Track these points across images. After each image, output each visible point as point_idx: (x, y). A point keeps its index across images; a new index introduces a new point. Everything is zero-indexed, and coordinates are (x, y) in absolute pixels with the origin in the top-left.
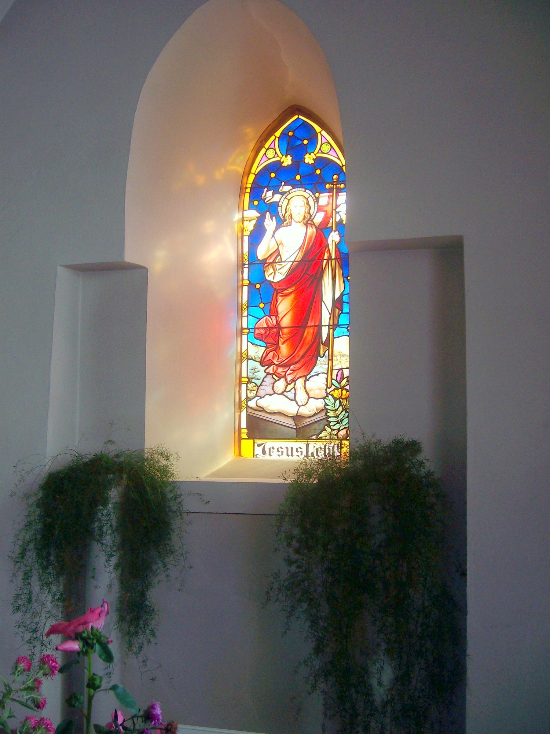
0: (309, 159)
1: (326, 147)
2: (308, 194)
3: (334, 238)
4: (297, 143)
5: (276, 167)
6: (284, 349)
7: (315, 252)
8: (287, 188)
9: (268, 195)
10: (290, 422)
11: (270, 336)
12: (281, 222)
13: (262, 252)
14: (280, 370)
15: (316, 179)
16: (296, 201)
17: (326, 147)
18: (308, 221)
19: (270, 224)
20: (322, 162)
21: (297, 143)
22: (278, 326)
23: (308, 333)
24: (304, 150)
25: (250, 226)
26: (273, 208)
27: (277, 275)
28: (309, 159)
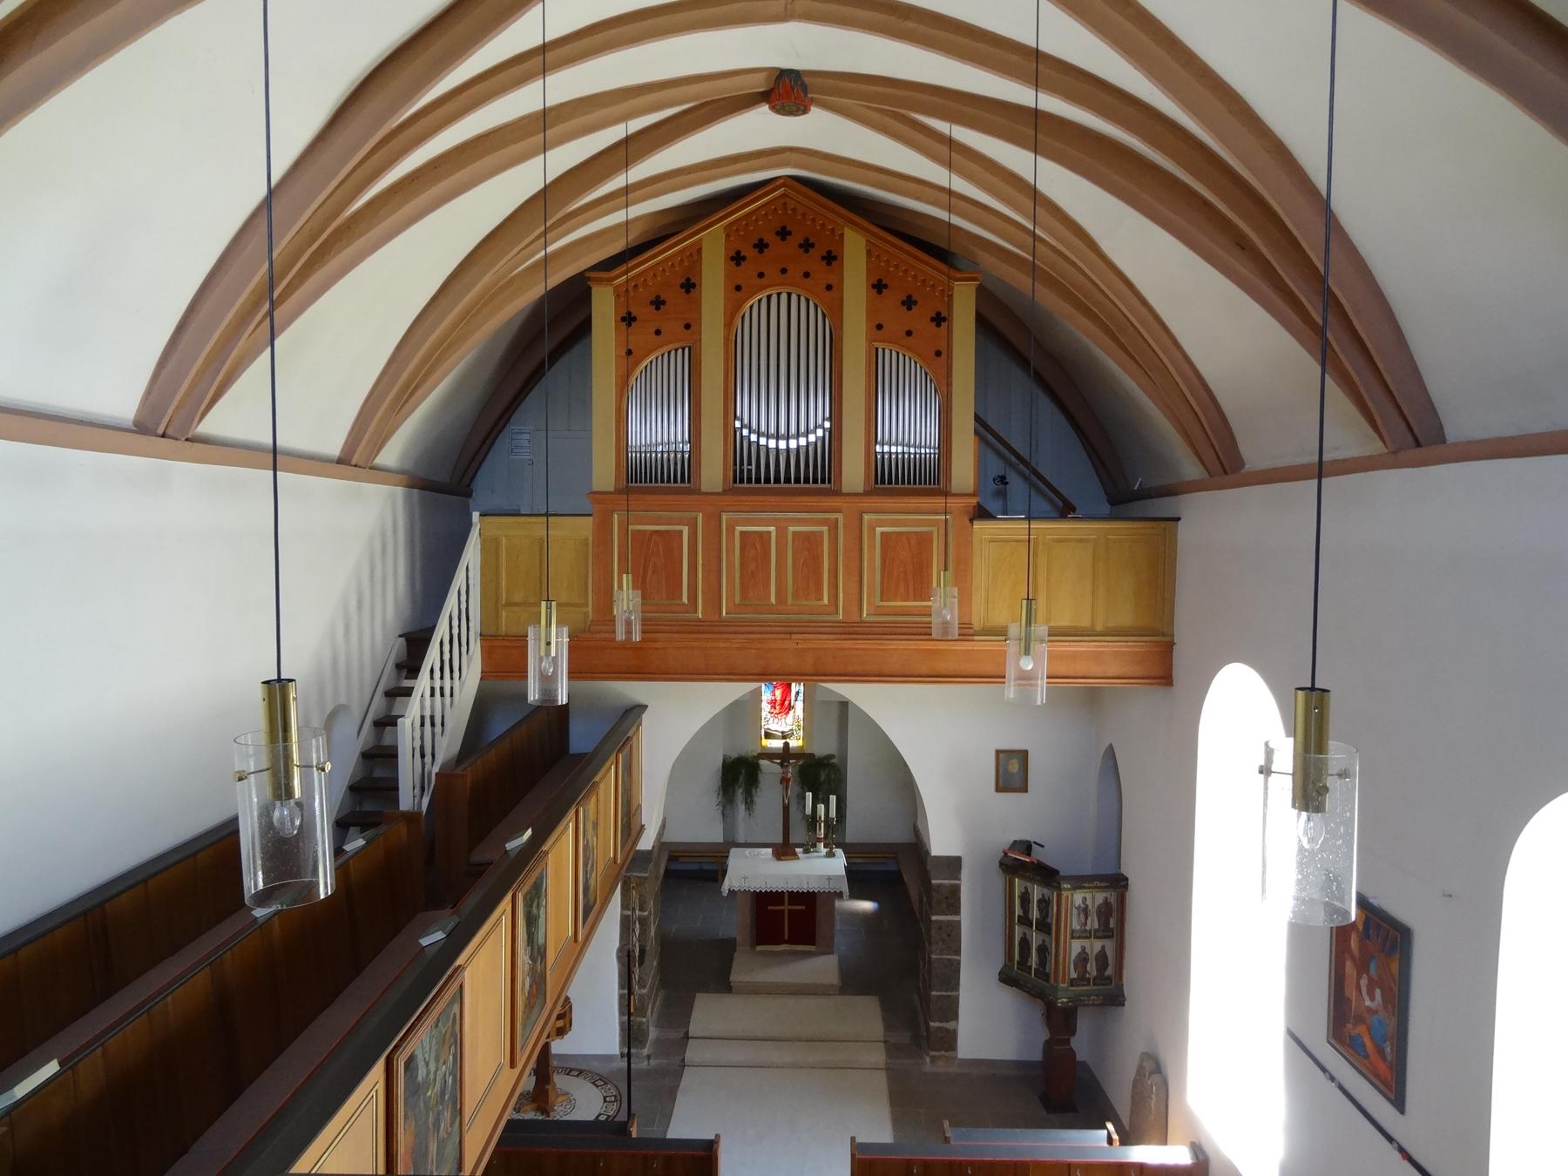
11: (773, 703)
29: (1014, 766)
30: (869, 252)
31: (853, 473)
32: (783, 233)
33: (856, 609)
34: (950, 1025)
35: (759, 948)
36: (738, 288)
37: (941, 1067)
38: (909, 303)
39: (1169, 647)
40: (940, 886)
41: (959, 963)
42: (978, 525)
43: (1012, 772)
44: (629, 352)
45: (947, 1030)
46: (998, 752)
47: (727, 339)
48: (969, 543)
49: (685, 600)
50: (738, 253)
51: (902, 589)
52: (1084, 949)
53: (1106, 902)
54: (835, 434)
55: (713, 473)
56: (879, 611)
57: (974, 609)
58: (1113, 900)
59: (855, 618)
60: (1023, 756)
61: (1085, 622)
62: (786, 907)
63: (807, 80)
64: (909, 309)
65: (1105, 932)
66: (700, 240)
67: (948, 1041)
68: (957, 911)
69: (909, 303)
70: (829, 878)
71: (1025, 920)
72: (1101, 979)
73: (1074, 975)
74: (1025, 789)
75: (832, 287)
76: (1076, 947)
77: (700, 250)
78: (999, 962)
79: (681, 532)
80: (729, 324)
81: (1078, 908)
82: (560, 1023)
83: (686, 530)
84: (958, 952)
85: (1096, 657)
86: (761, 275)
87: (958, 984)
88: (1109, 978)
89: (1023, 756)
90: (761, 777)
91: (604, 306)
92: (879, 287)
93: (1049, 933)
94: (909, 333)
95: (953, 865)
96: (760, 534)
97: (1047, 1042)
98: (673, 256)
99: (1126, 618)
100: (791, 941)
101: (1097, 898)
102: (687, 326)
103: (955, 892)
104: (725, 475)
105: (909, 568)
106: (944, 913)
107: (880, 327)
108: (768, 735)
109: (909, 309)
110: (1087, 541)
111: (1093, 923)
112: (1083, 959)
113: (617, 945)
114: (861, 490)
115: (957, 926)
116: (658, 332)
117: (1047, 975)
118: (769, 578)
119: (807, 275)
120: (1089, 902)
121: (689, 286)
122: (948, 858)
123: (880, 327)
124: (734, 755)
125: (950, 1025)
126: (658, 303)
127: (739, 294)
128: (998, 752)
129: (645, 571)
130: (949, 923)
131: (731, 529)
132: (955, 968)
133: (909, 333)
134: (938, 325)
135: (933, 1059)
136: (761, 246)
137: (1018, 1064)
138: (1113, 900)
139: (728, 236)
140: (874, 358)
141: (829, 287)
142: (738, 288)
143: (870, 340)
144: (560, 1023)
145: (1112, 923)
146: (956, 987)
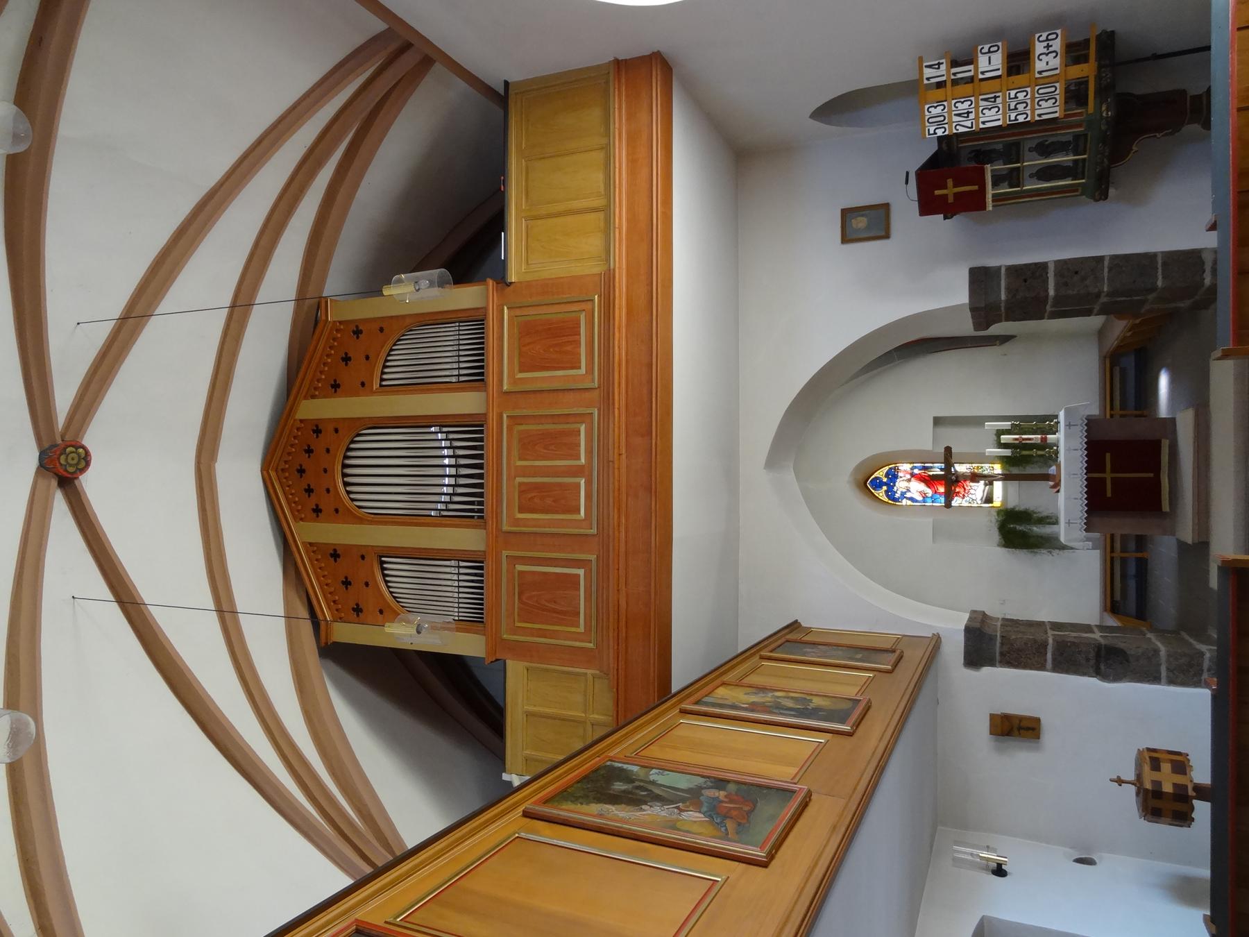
0: (885, 480)
1: (881, 474)
3: (916, 471)
4: (878, 484)
5: (886, 492)
7: (922, 479)
9: (897, 495)
12: (909, 491)
13: (920, 498)
15: (893, 476)
16: (900, 485)
17: (881, 474)
18: (909, 480)
19: (908, 495)
20: (887, 475)
21: (878, 484)
24: (881, 481)
25: (909, 503)
26: (903, 494)
27: (929, 492)
28: (885, 480)
29: (860, 223)
30: (313, 397)
31: (465, 403)
32: (301, 471)
33: (587, 395)
35: (1166, 507)
36: (337, 511)
38: (346, 359)
39: (619, 65)
40: (1008, 289)
42: (513, 277)
43: (865, 224)
44: (381, 612)
46: (845, 240)
47: (371, 522)
48: (529, 285)
49: (581, 572)
50: (314, 510)
51: (569, 348)
54: (442, 421)
55: (467, 538)
56: (590, 369)
57: (587, 272)
59: (596, 394)
60: (847, 214)
61: (599, 156)
62: (1108, 476)
63: (46, 445)
64: (349, 359)
66: (303, 543)
68: (1042, 267)
69: (346, 359)
70: (1069, 425)
71: (1013, 178)
74: (886, 207)
75: (338, 426)
77: (311, 544)
78: (1091, 210)
79: (521, 573)
80: (361, 520)
82: (1166, 767)
83: (520, 568)
84: (1100, 259)
85: (632, 139)
86: (328, 491)
90: (1022, 508)
91: (347, 633)
92: (336, 386)
93: (1017, 145)
94: (367, 358)
95: (980, 278)
96: (521, 492)
98: (312, 565)
99: (595, 114)
100: (1157, 468)
102: (363, 557)
103: (1014, 271)
104: (475, 527)
105: (549, 340)
107: (363, 384)
108: (989, 499)
109: (349, 359)
110: (527, 168)
113: (1094, 681)
114: (483, 394)
115: (1062, 265)
116: (367, 584)
117: (1077, 137)
118: (560, 485)
119: (328, 451)
121: (335, 555)
123: (363, 384)
124: (996, 536)
126: (347, 583)
127: (341, 510)
128: (845, 240)
129: (555, 611)
130: (1059, 274)
131: (517, 522)
132: (1121, 262)
133: (367, 358)
134: (361, 332)
136: (309, 491)
139: (302, 519)
140: (385, 389)
141: (336, 431)
142: (337, 511)
143: (372, 393)
144: (1166, 767)
146: (1150, 257)
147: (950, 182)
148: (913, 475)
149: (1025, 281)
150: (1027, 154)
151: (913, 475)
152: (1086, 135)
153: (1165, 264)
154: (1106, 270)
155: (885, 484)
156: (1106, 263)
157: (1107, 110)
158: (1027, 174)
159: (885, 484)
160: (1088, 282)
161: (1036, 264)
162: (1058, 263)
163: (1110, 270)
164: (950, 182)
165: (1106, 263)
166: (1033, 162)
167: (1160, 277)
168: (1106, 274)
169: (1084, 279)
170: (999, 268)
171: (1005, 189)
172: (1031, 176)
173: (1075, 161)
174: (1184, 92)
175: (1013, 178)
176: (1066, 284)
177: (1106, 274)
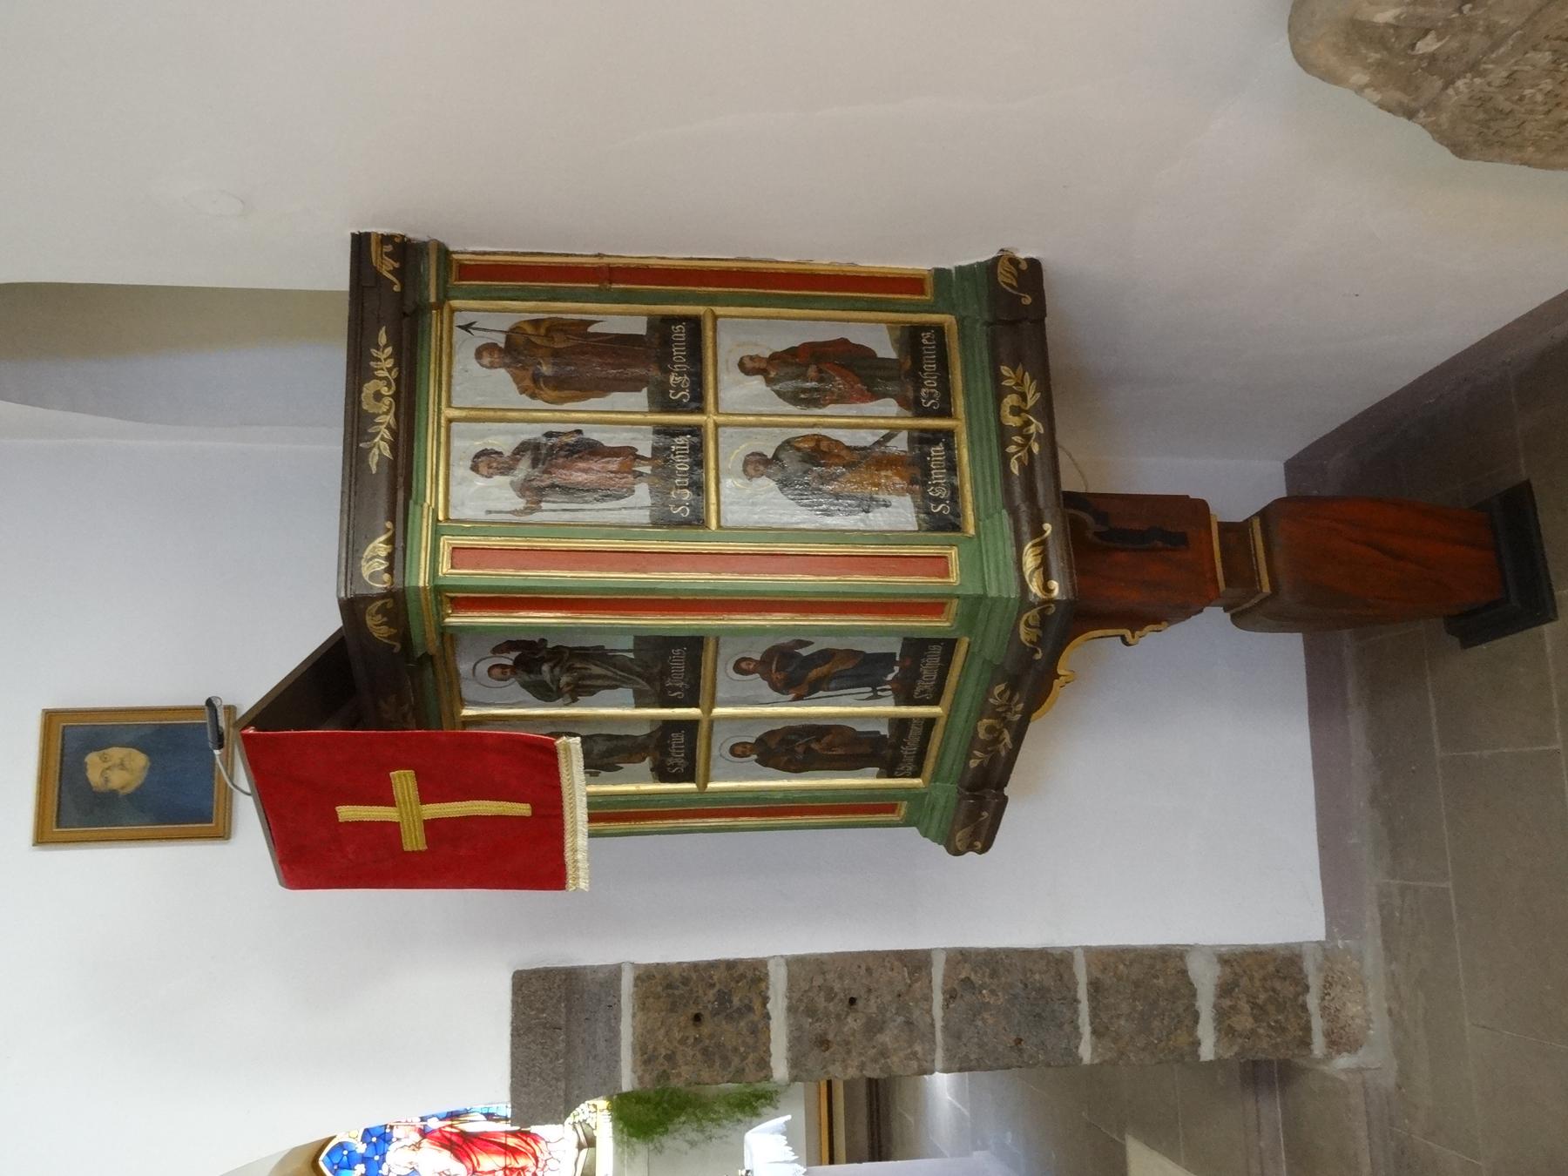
2: (392, 1148)
6: (522, 1162)
8: (385, 1167)
10: (585, 1151)
14: (541, 1165)
18: (417, 1146)
22: (505, 1168)
23: (512, 1142)
28: (361, 1148)
34: (1205, 977)
37: (1369, 1009)
40: (646, 1056)
41: (960, 957)
45: (1225, 989)
52: (757, 464)
53: (515, 352)
58: (497, 318)
65: (668, 357)
67: (1265, 979)
68: (751, 975)
71: (673, 751)
72: (916, 369)
73: (898, 512)
76: (746, 502)
81: (534, 493)
84: (916, 962)
87: (1043, 954)
88: (911, 338)
89: (71, 741)
93: (694, 645)
97: (1241, 617)
101: (479, 399)
106: (760, 1031)
111: (621, 417)
112: (551, 461)
115: (805, 969)
117: (916, 646)
120: (504, 440)
122: (520, 1031)
125: (1205, 977)
135: (1339, 1041)
137: (1324, 702)
138: (497, 318)
145: (625, 331)
146: (1057, 961)
147: (403, 782)
148: (424, 1133)
149: (697, 1018)
150: (727, 679)
151: (424, 1133)
152: (949, 645)
153: (1095, 987)
154: (938, 998)
155: (365, 1159)
156: (938, 973)
157: (1044, 567)
158: (722, 742)
159: (365, 1159)
160: (885, 1038)
161: (730, 965)
162: (799, 966)
163: (950, 996)
164: (403, 782)
165: (938, 973)
166: (743, 706)
167: (1086, 1030)
168: (938, 1012)
169: (873, 1027)
170: (615, 972)
171: (637, 783)
172: (739, 751)
173: (900, 724)
174: (1198, 509)
175: (673, 751)
176: (823, 1043)
177: (938, 1012)
